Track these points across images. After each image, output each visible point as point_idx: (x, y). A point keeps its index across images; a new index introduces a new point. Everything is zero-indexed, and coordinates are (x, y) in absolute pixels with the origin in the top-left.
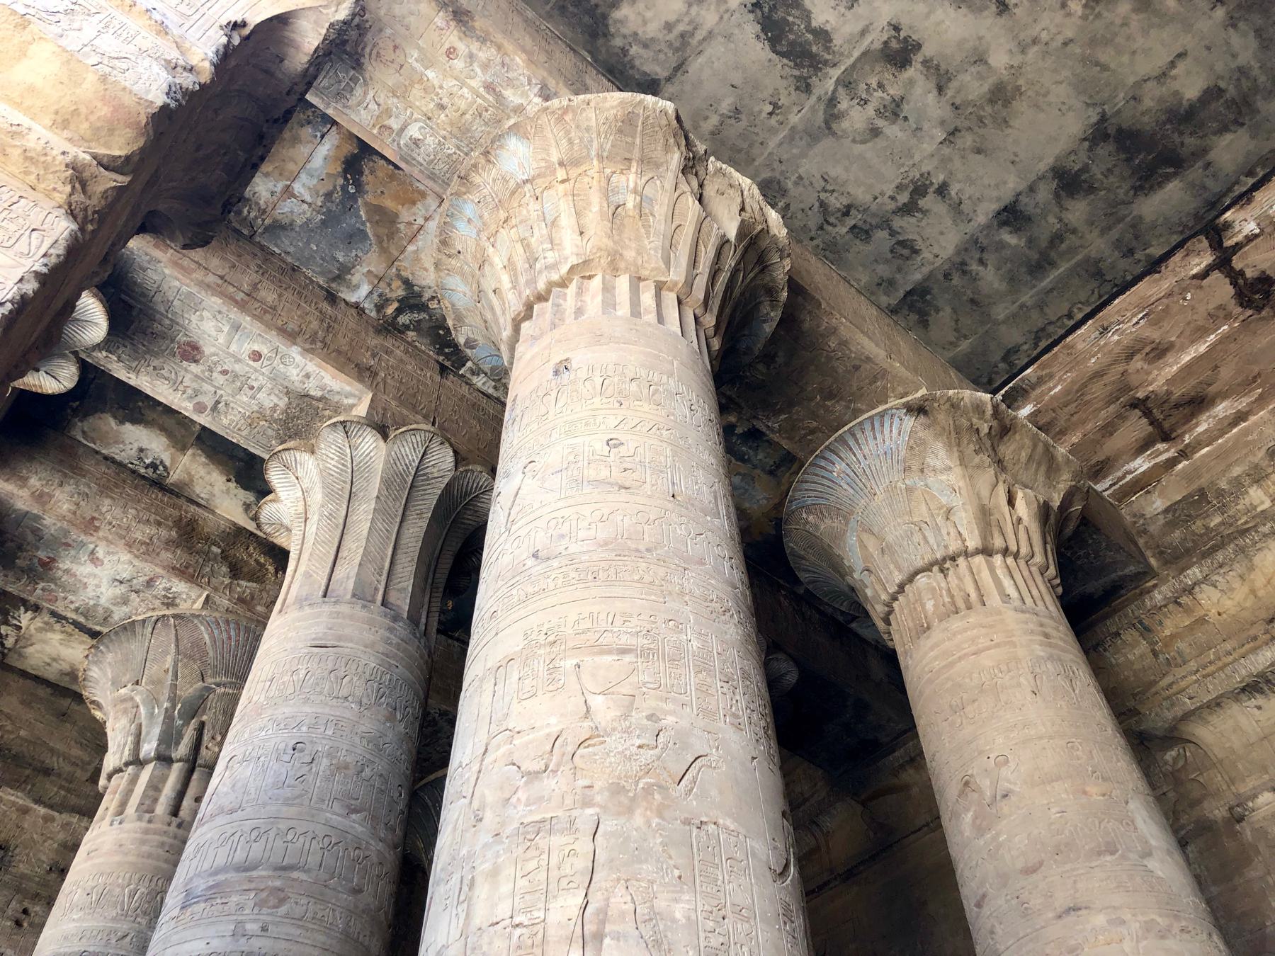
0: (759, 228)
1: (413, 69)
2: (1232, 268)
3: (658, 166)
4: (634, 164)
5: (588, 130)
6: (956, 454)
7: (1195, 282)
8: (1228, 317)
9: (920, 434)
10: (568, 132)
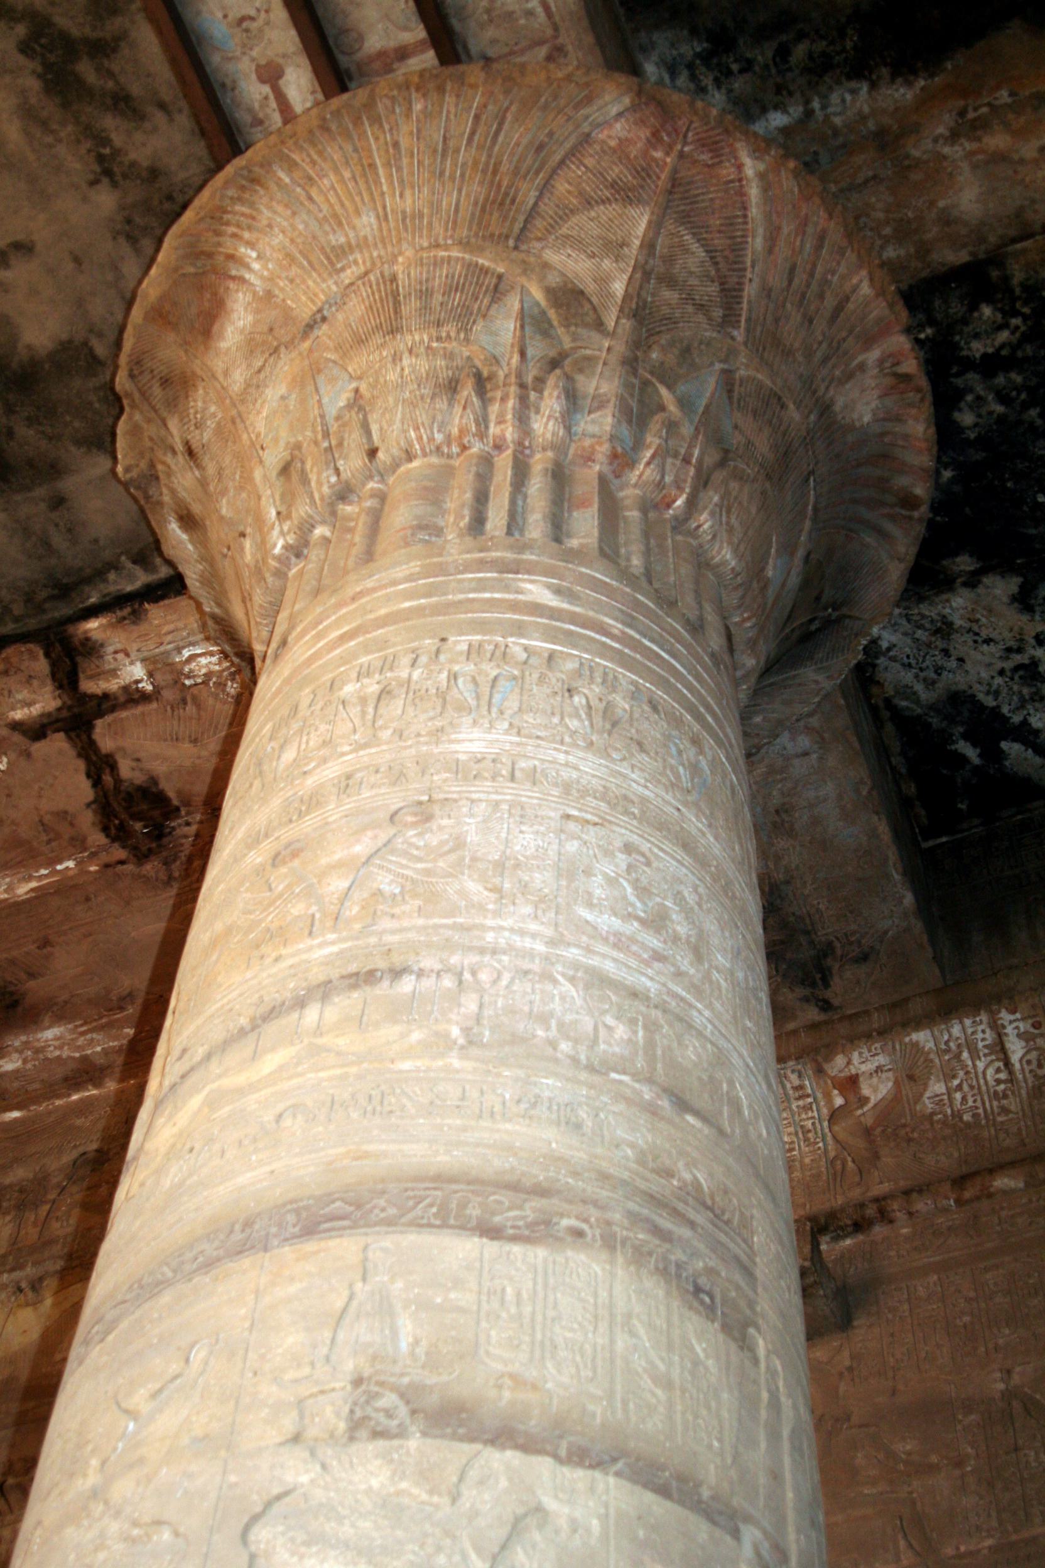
2: (92, 743)
7: (17, 738)
8: (78, 843)
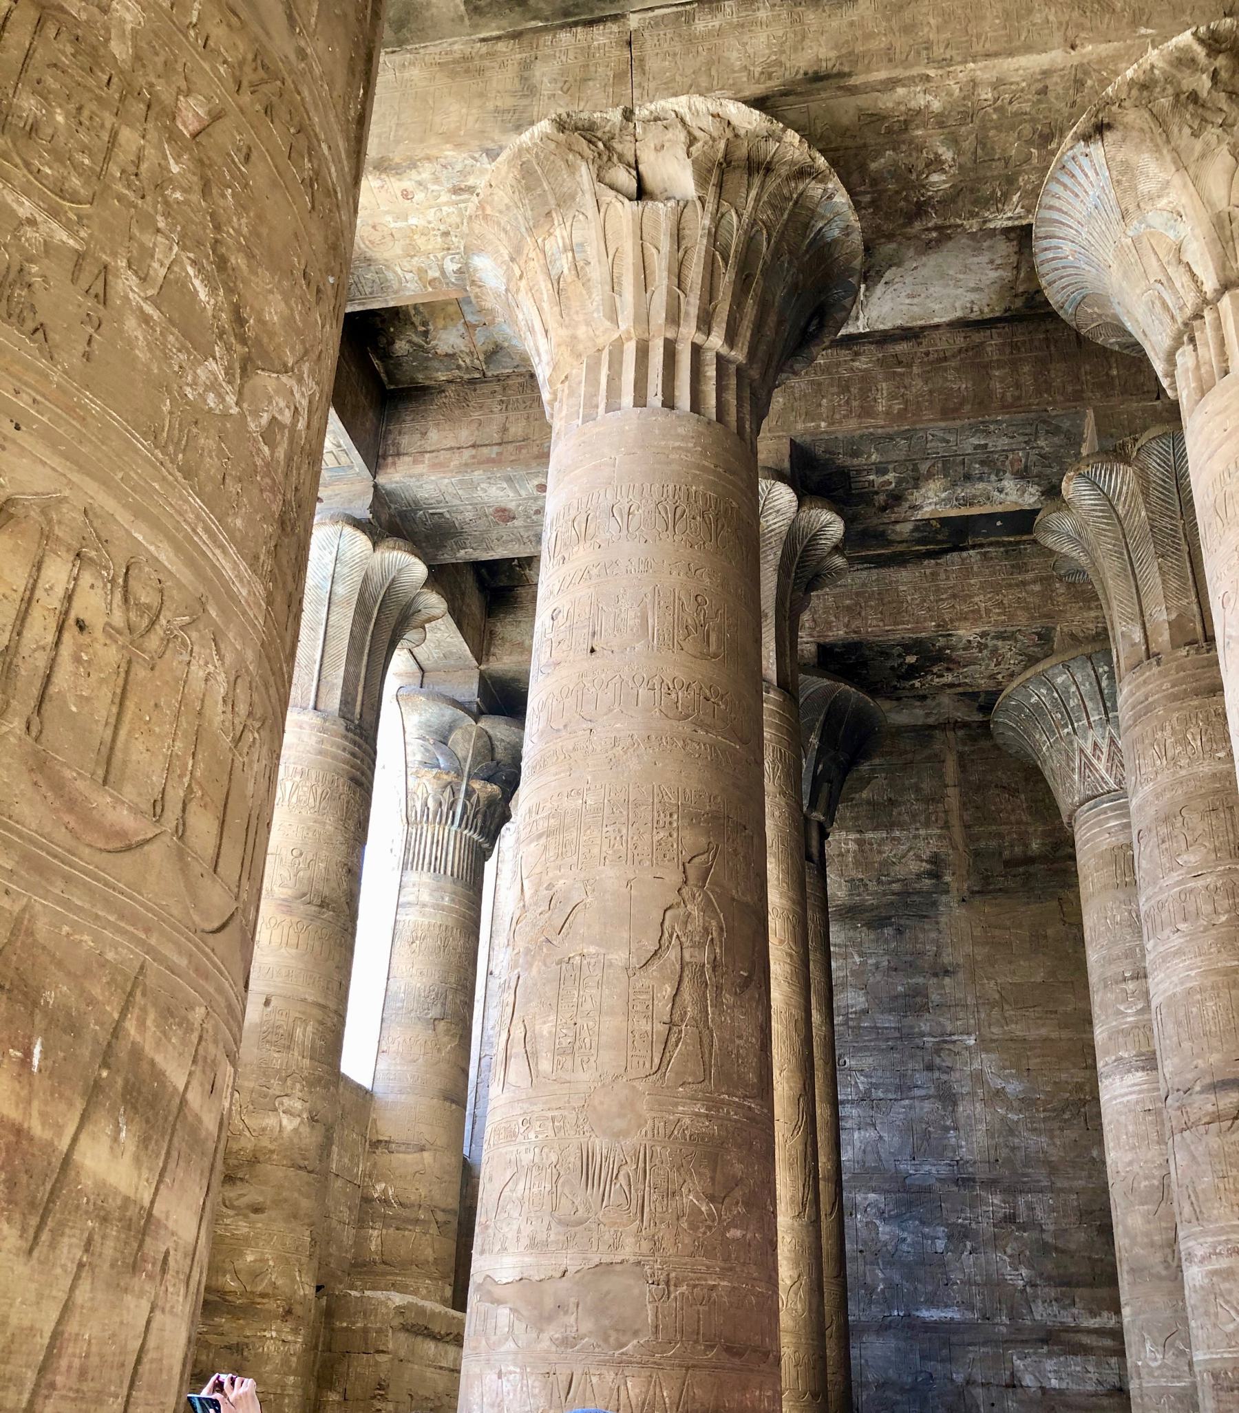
0: (722, 145)
1: (400, 229)
3: (573, 197)
4: (554, 215)
5: (508, 208)
6: (1168, 158)
9: (1120, 157)
10: (499, 224)
